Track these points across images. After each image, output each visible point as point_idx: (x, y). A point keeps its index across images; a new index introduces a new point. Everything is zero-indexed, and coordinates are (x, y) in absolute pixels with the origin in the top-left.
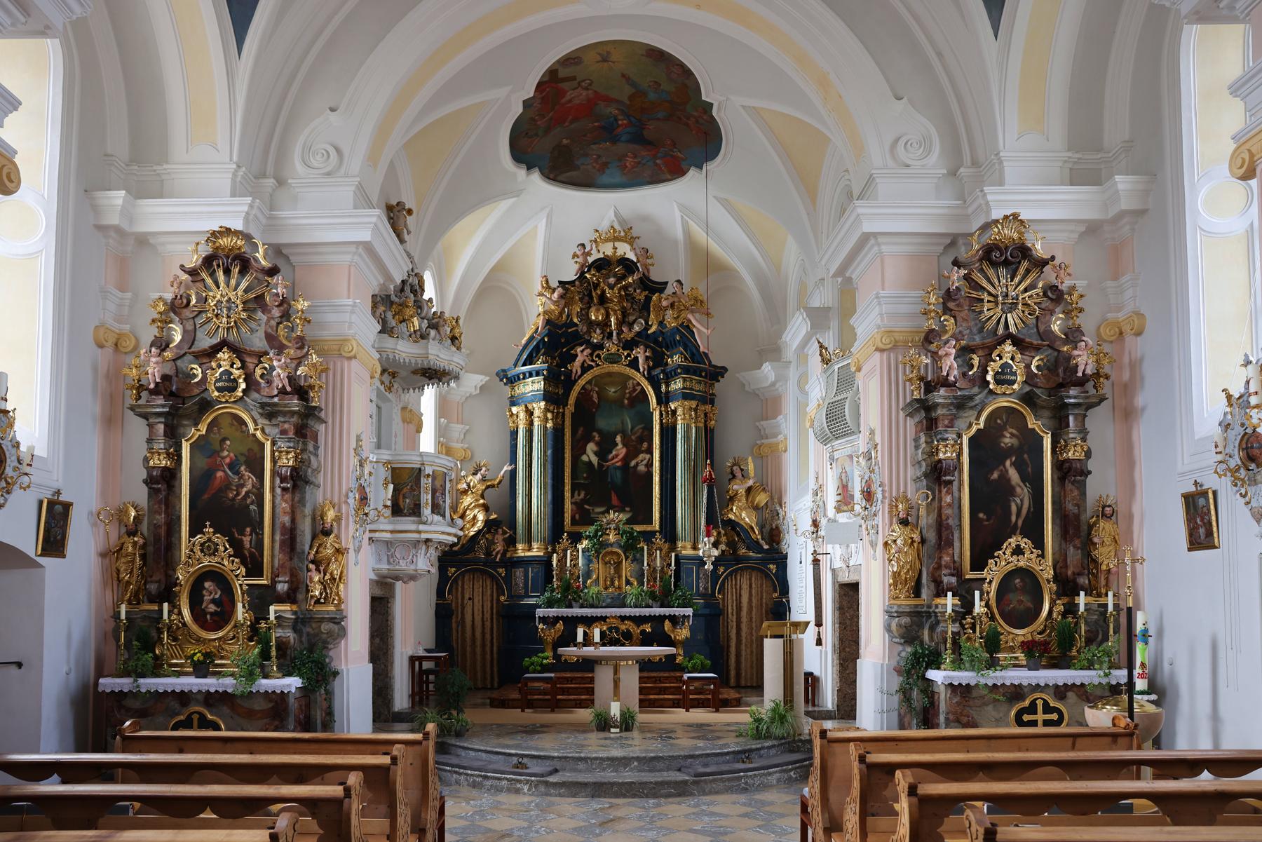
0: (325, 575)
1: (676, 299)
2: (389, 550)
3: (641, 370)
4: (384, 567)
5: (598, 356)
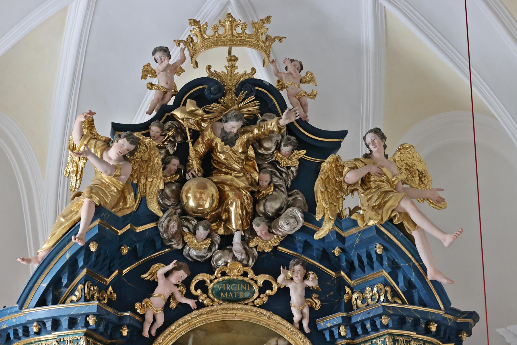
1: (374, 170)
3: (297, 317)
5: (202, 286)
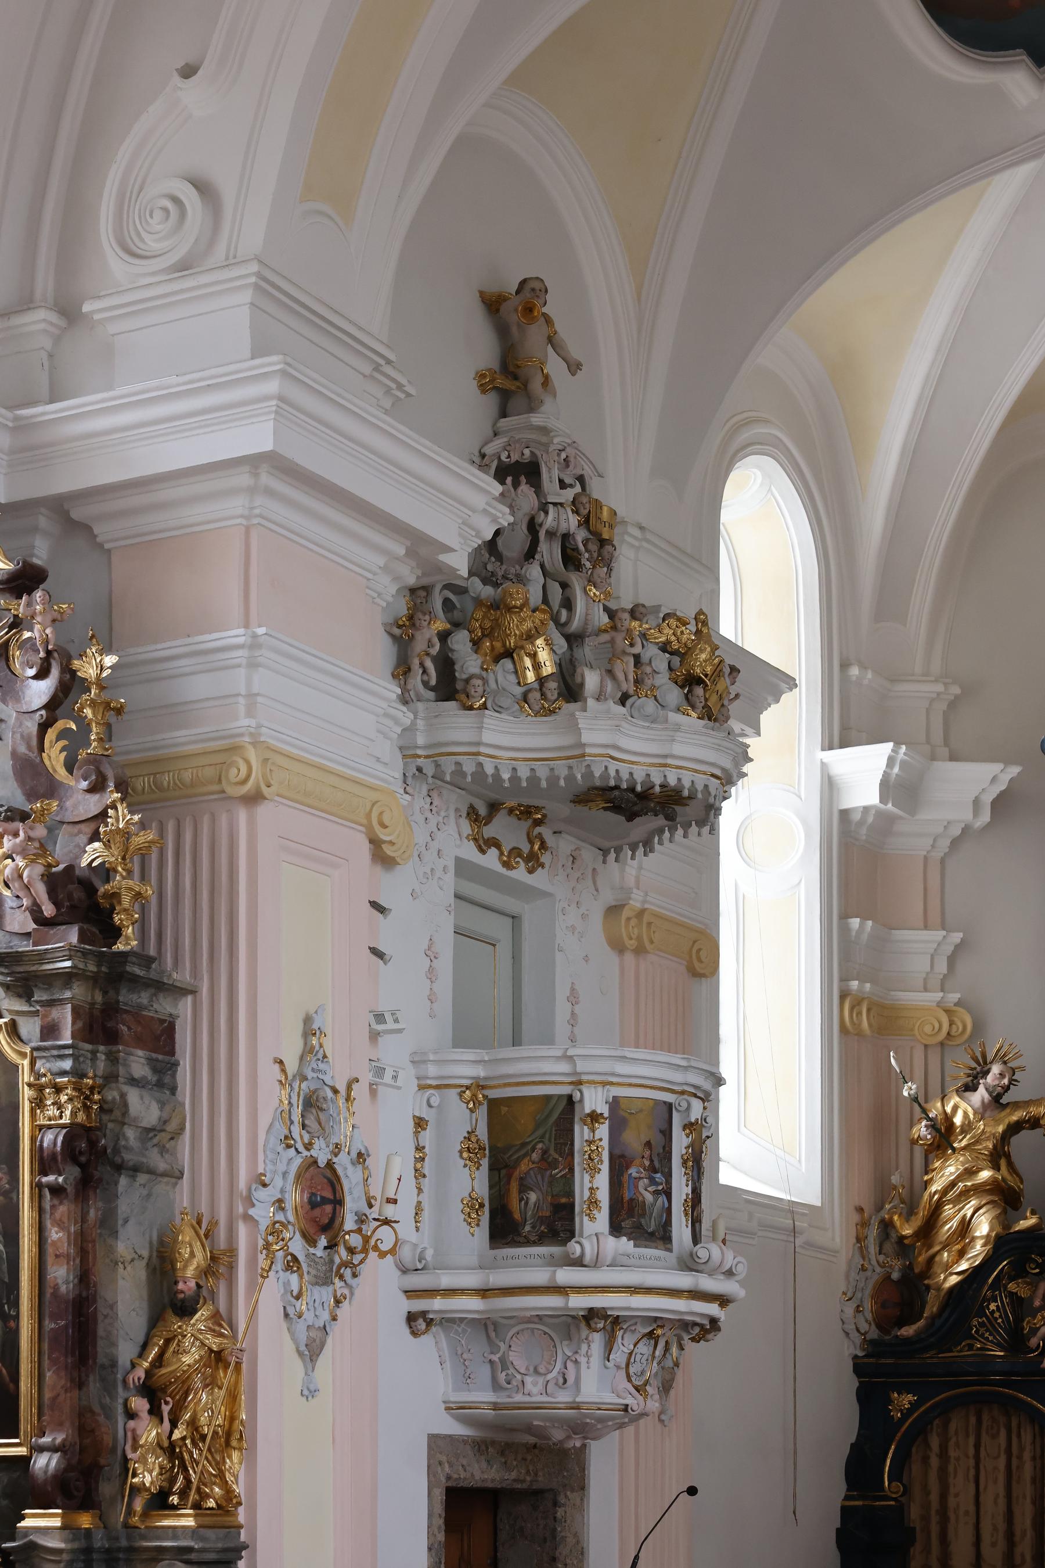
0: (174, 1425)
2: (494, 1348)
4: (483, 1396)
